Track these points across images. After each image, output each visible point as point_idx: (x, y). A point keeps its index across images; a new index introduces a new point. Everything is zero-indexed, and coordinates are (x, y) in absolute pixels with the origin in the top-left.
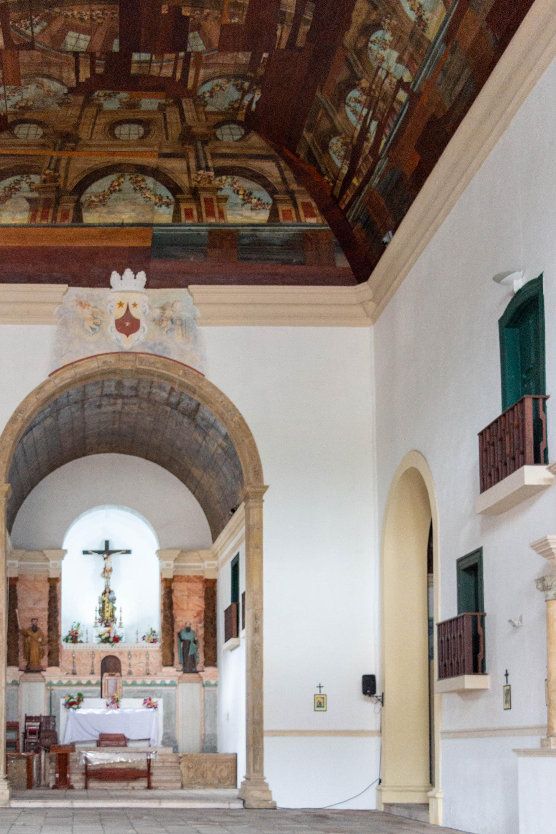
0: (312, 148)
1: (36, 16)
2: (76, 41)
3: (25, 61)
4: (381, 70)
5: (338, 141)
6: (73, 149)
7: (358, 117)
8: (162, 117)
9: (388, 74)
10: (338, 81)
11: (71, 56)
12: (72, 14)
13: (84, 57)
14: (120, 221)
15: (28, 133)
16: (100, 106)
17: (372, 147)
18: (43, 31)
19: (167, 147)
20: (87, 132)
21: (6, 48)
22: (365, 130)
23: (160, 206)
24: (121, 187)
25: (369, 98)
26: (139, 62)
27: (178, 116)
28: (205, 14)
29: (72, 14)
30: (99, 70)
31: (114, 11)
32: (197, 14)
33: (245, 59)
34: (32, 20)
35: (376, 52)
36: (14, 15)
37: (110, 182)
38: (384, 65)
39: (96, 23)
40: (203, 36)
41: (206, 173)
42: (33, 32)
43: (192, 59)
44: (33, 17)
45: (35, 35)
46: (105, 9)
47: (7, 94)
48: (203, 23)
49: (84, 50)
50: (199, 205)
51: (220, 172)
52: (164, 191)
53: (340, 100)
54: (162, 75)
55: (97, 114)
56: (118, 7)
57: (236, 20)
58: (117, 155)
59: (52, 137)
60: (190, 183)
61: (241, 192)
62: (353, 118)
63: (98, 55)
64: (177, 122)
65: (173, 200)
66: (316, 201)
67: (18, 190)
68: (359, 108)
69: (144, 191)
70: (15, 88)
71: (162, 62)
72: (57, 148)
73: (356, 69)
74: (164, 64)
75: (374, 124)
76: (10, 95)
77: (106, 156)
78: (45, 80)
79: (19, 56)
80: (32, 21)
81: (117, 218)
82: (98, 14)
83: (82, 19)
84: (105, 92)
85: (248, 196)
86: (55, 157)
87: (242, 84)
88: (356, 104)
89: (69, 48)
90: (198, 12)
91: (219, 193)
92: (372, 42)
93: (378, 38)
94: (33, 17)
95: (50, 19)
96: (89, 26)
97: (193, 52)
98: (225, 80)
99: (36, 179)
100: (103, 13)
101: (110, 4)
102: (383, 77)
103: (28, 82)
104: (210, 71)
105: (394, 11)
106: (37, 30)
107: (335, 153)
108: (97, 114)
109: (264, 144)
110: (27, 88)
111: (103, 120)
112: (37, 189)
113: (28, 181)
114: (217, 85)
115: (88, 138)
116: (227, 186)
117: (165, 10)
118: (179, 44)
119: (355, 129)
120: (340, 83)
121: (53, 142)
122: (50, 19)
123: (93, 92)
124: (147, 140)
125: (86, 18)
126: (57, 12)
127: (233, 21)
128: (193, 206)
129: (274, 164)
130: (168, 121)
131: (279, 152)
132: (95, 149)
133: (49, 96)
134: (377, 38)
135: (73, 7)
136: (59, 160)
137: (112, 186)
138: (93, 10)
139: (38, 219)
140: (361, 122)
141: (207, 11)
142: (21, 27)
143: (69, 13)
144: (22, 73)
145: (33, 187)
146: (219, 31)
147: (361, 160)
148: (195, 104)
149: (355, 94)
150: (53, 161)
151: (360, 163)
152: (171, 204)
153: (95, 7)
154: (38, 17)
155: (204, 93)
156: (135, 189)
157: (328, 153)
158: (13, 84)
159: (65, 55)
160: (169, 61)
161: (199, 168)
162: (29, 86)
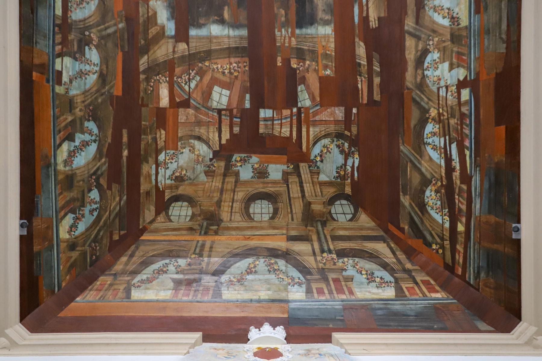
0: (413, 214)
1: (192, 71)
2: (220, 97)
3: (183, 121)
4: (441, 89)
5: (431, 191)
6: (216, 233)
7: (439, 152)
8: (286, 189)
9: (447, 87)
10: (412, 126)
11: (216, 114)
12: (217, 68)
13: (225, 115)
14: (257, 298)
15: (181, 212)
16: (237, 174)
17: (461, 173)
18: (197, 86)
19: (293, 229)
20: (228, 212)
21: (171, 106)
22: (448, 160)
23: (293, 286)
24: (256, 269)
25: (441, 124)
26: (265, 120)
27: (299, 188)
28: (307, 65)
29: (217, 68)
30: (236, 130)
31: (245, 64)
32: (301, 66)
33: (341, 114)
34: (190, 74)
35: (432, 77)
36: (178, 70)
37: (247, 265)
38: (442, 83)
39: (233, 77)
40: (308, 88)
41: (330, 255)
42: (190, 87)
43: (303, 115)
44: (191, 72)
45: (191, 90)
46: (239, 62)
47: (167, 160)
48: (307, 76)
49: (225, 107)
50: (328, 285)
51: (341, 254)
52: (295, 273)
53: (419, 145)
54: (282, 135)
55: (235, 186)
56: (247, 59)
57: (328, 72)
58: (252, 239)
59: (199, 218)
60: (317, 266)
61: (363, 273)
62: (435, 155)
63: (235, 111)
64: (299, 198)
65: (304, 280)
66: (432, 278)
67: (166, 272)
68: (436, 139)
69: (277, 273)
70: (174, 153)
71: (281, 120)
72: (203, 232)
73: (422, 103)
74: (283, 121)
75: (454, 146)
76: (169, 161)
77: (243, 240)
78: (196, 143)
79: (178, 116)
80: (189, 76)
81: (254, 295)
82: (235, 67)
83: (224, 73)
84: (241, 155)
85: (371, 278)
86: (200, 242)
87: (343, 144)
88: (433, 138)
89: (215, 105)
90: (301, 64)
91: (344, 273)
92: (426, 70)
93: (430, 62)
94: (191, 72)
95: (201, 73)
96: (228, 80)
97: (303, 108)
98: (329, 139)
99: (182, 262)
100: (238, 67)
101: (242, 57)
102: (445, 95)
103: (184, 146)
104: (317, 129)
105: (434, 31)
106: (193, 84)
107: (432, 208)
108: (235, 186)
109: (372, 224)
110: (182, 153)
111: (240, 195)
112: (182, 272)
113: (176, 264)
114: (324, 146)
115: (229, 219)
116: (349, 266)
117: (279, 64)
118: (292, 99)
119: (440, 166)
120: (415, 126)
121: (199, 225)
122: (201, 73)
123: (231, 156)
124: (277, 221)
125: (226, 71)
126: (207, 66)
127: (327, 73)
128: (323, 286)
129: (385, 245)
130: (291, 195)
131: (387, 231)
132: (234, 233)
133: (198, 162)
134: (428, 63)
135: (219, 61)
136: (203, 246)
137: (248, 268)
138: (231, 64)
139: (180, 296)
140: (443, 155)
141: (308, 62)
142: (182, 82)
143: (215, 67)
144: (180, 135)
145: (179, 270)
146: (319, 85)
147: (457, 197)
148: (311, 172)
149: (430, 128)
150: (199, 245)
151: (457, 201)
152: (302, 284)
153: (232, 60)
154: (194, 71)
155: (316, 156)
156: (269, 271)
157: (427, 212)
158: (172, 150)
159: (211, 113)
160: (286, 118)
161: (323, 251)
162: (184, 150)
